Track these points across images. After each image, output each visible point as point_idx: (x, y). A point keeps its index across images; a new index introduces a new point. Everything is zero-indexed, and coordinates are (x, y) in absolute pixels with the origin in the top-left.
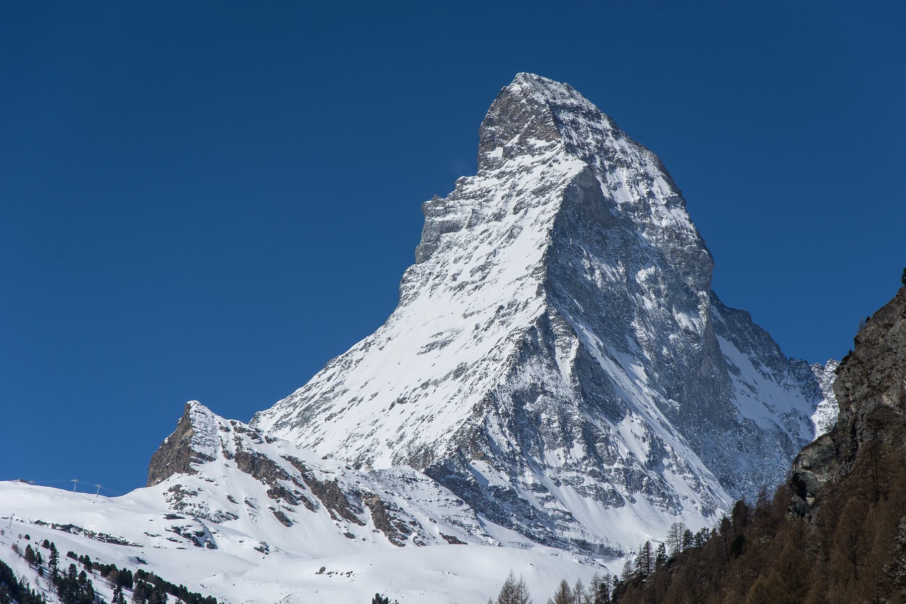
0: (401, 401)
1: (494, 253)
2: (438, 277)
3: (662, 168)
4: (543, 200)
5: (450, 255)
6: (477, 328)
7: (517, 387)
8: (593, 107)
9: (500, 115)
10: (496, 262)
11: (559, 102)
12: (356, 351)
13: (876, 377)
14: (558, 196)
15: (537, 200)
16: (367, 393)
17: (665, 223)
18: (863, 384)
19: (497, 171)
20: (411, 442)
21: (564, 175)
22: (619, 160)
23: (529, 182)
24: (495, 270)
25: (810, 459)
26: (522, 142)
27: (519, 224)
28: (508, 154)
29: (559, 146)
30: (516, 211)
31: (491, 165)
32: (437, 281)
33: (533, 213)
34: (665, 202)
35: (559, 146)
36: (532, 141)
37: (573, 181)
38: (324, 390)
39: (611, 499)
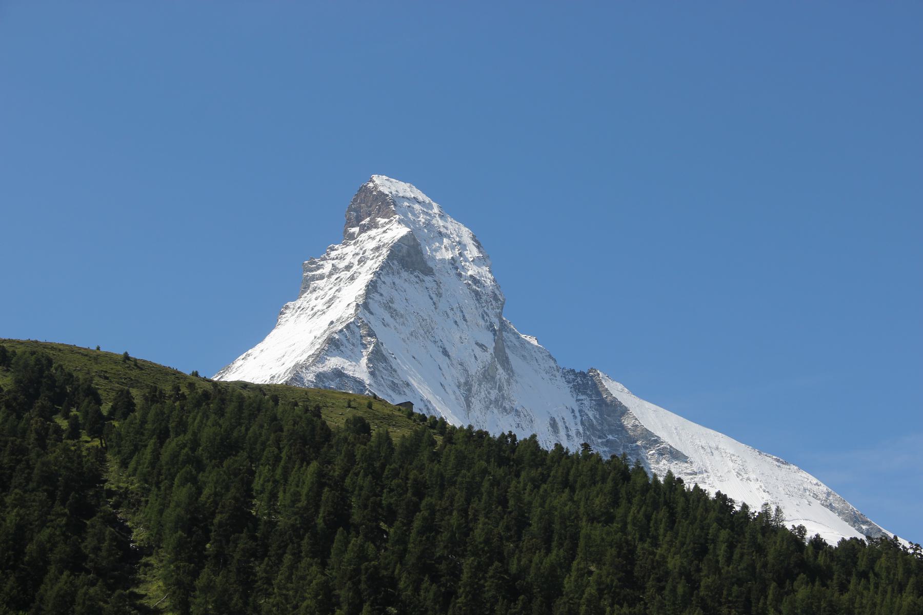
3: (474, 238)
4: (377, 254)
5: (315, 295)
7: (321, 370)
8: (427, 200)
11: (401, 195)
17: (470, 273)
22: (440, 233)
23: (373, 244)
24: (338, 300)
28: (364, 229)
30: (360, 262)
31: (352, 237)
33: (369, 263)
36: (379, 219)
37: (399, 241)
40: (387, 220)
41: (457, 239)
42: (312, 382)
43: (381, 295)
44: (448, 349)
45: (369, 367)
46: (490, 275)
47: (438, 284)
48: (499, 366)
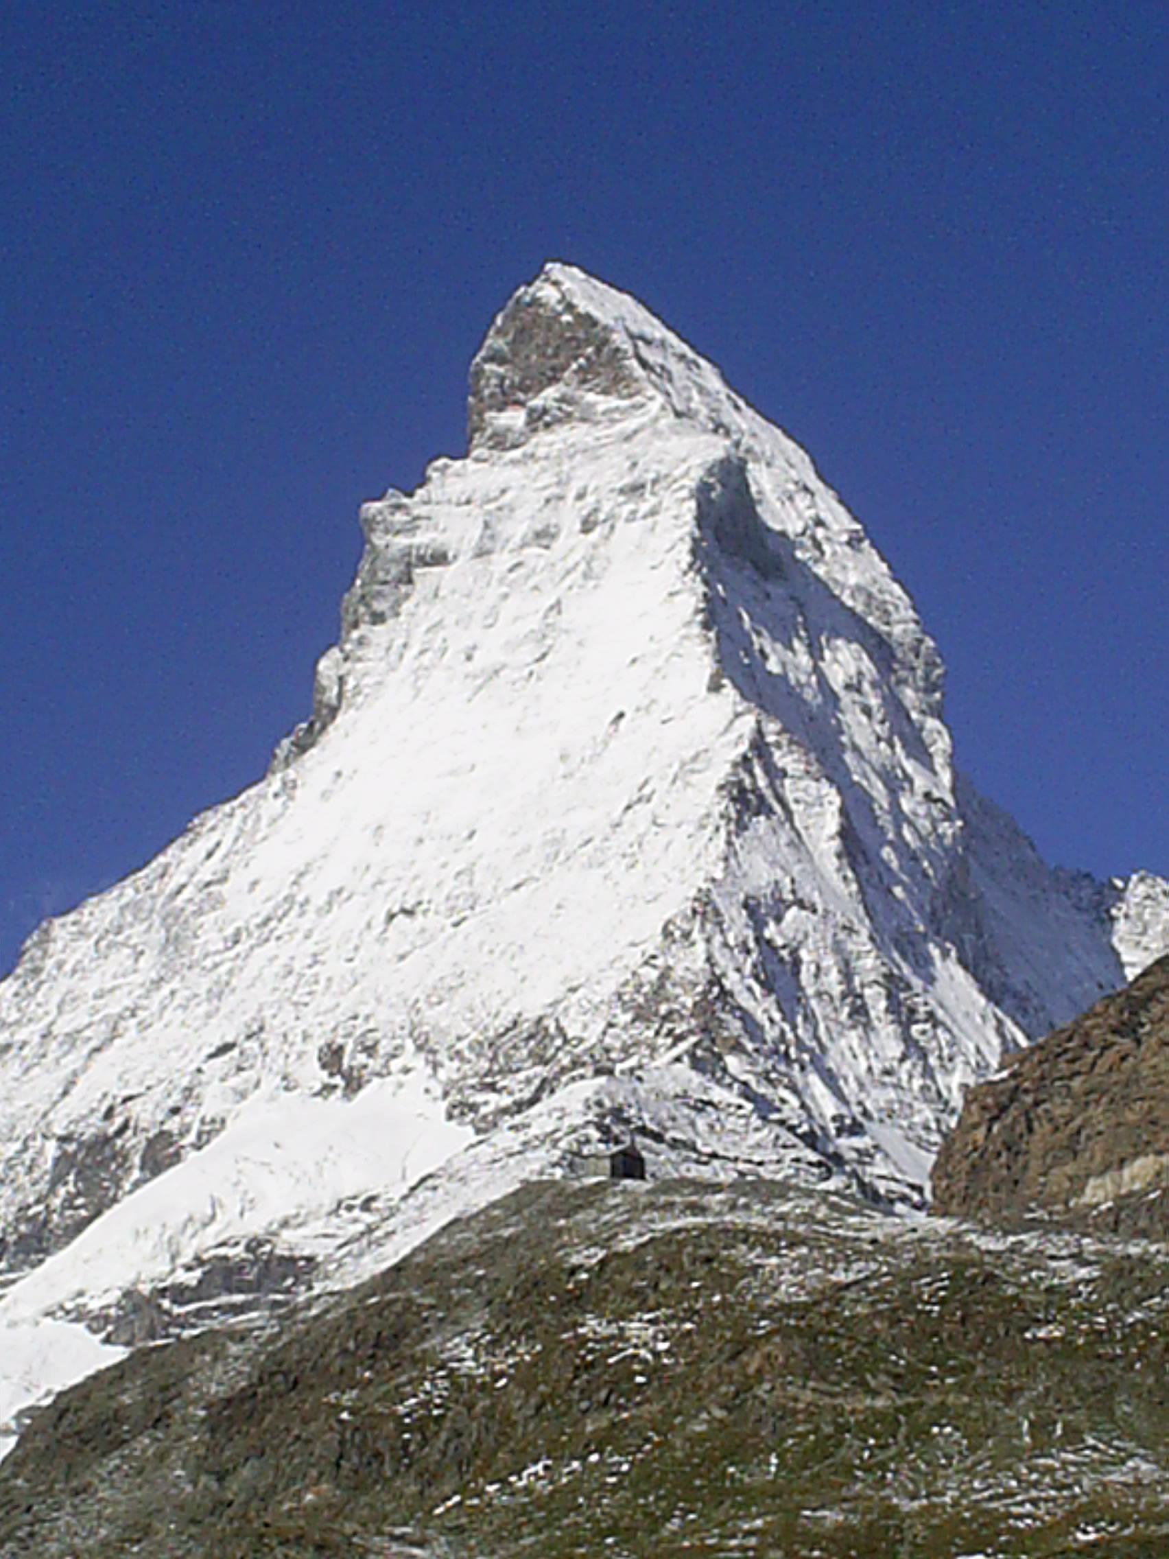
1: (557, 606)
2: (422, 652)
4: (644, 508)
9: (514, 341)
10: (564, 626)
12: (262, 799)
15: (631, 506)
16: (316, 889)
19: (516, 454)
21: (684, 460)
30: (587, 526)
31: (501, 442)
32: (426, 659)
34: (845, 538)
37: (710, 472)
38: (205, 875)
46: (896, 588)
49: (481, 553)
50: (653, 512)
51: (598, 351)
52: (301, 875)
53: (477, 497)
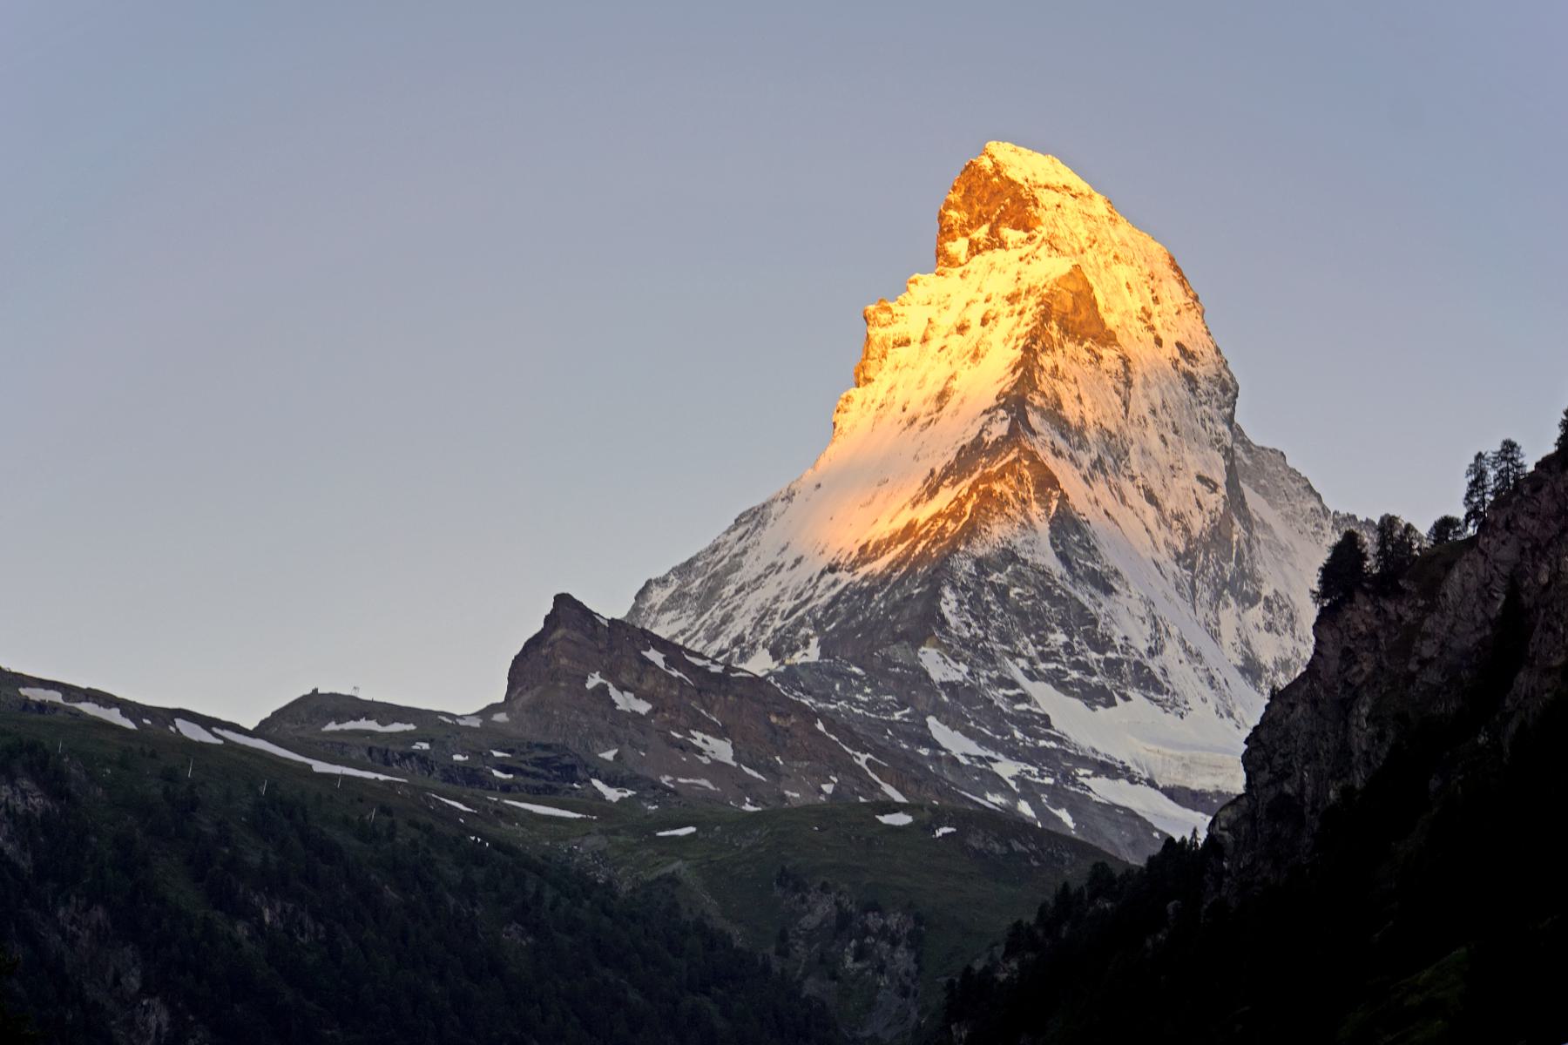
0: (832, 569)
1: (953, 377)
4: (1018, 307)
6: (932, 472)
8: (1085, 187)
11: (1042, 182)
13: (1278, 761)
14: (1038, 305)
18: (1263, 769)
19: (959, 270)
20: (847, 621)
22: (1116, 257)
23: (1002, 285)
25: (1228, 820)
26: (993, 231)
27: (989, 338)
28: (975, 249)
29: (1039, 237)
30: (984, 322)
31: (951, 262)
33: (1005, 325)
35: (1039, 237)
38: (735, 550)
39: (1096, 697)
40: (1024, 235)
41: (1147, 270)
42: (971, 575)
43: (1043, 394)
44: (1156, 493)
45: (1054, 545)
47: (1126, 361)
48: (1236, 521)
49: (925, 340)
50: (1021, 313)
51: (1013, 202)
52: (784, 549)
53: (934, 301)
